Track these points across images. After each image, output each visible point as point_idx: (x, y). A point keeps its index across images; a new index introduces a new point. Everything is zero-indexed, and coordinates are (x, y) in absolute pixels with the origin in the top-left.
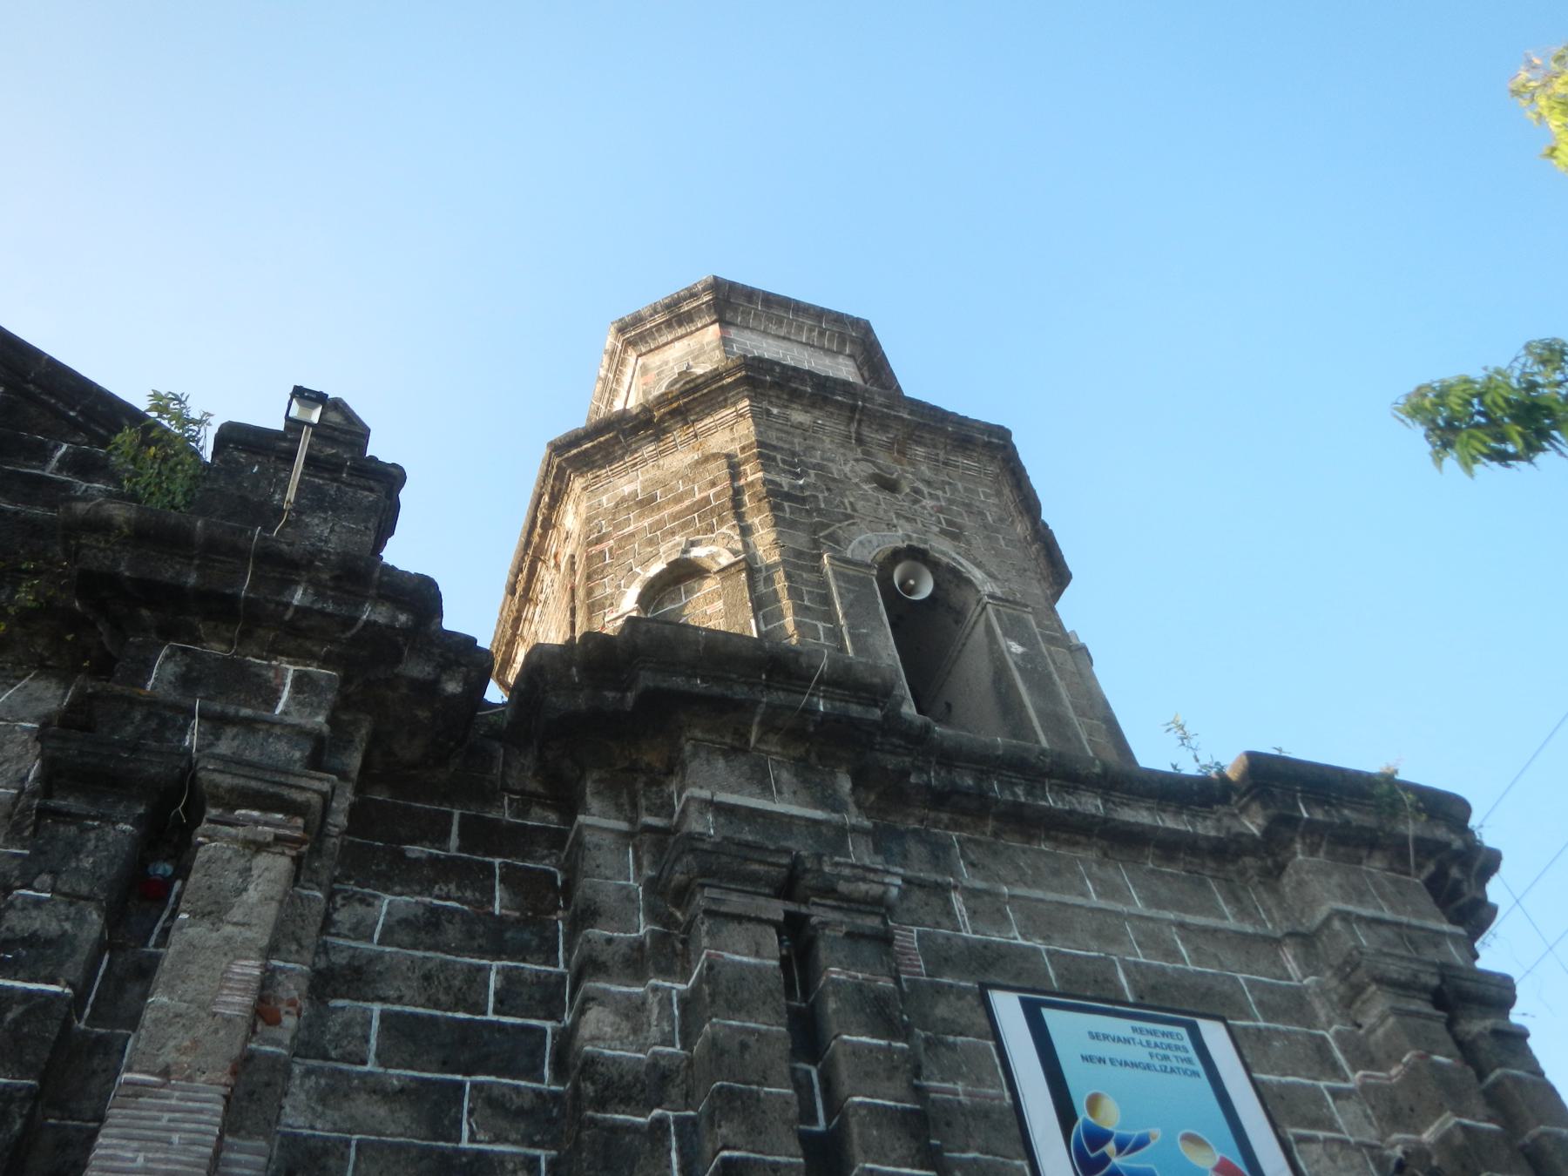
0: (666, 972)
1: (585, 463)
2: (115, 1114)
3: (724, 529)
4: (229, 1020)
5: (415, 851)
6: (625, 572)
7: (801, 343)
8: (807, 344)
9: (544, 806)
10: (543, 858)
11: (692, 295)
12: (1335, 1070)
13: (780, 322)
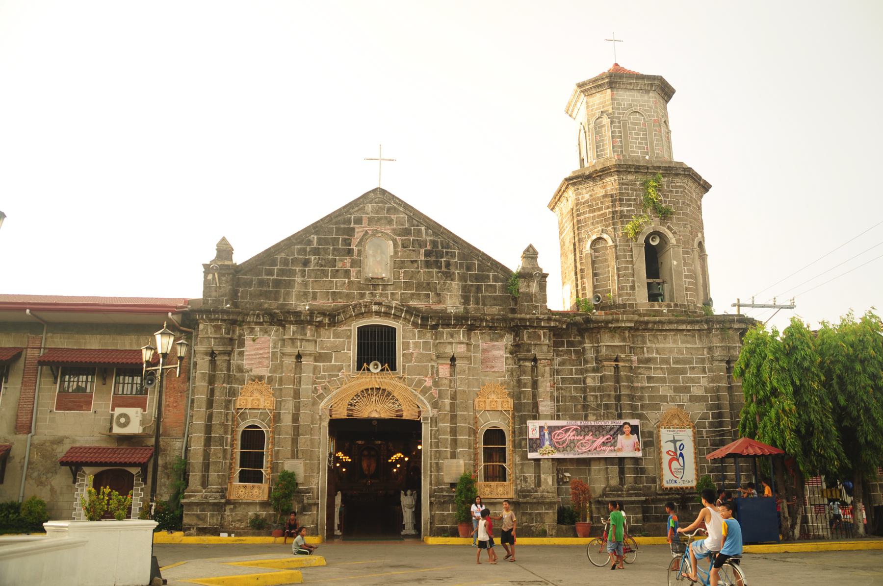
0: (598, 373)
1: (574, 184)
3: (610, 228)
11: (601, 78)
12: (705, 373)
13: (631, 84)
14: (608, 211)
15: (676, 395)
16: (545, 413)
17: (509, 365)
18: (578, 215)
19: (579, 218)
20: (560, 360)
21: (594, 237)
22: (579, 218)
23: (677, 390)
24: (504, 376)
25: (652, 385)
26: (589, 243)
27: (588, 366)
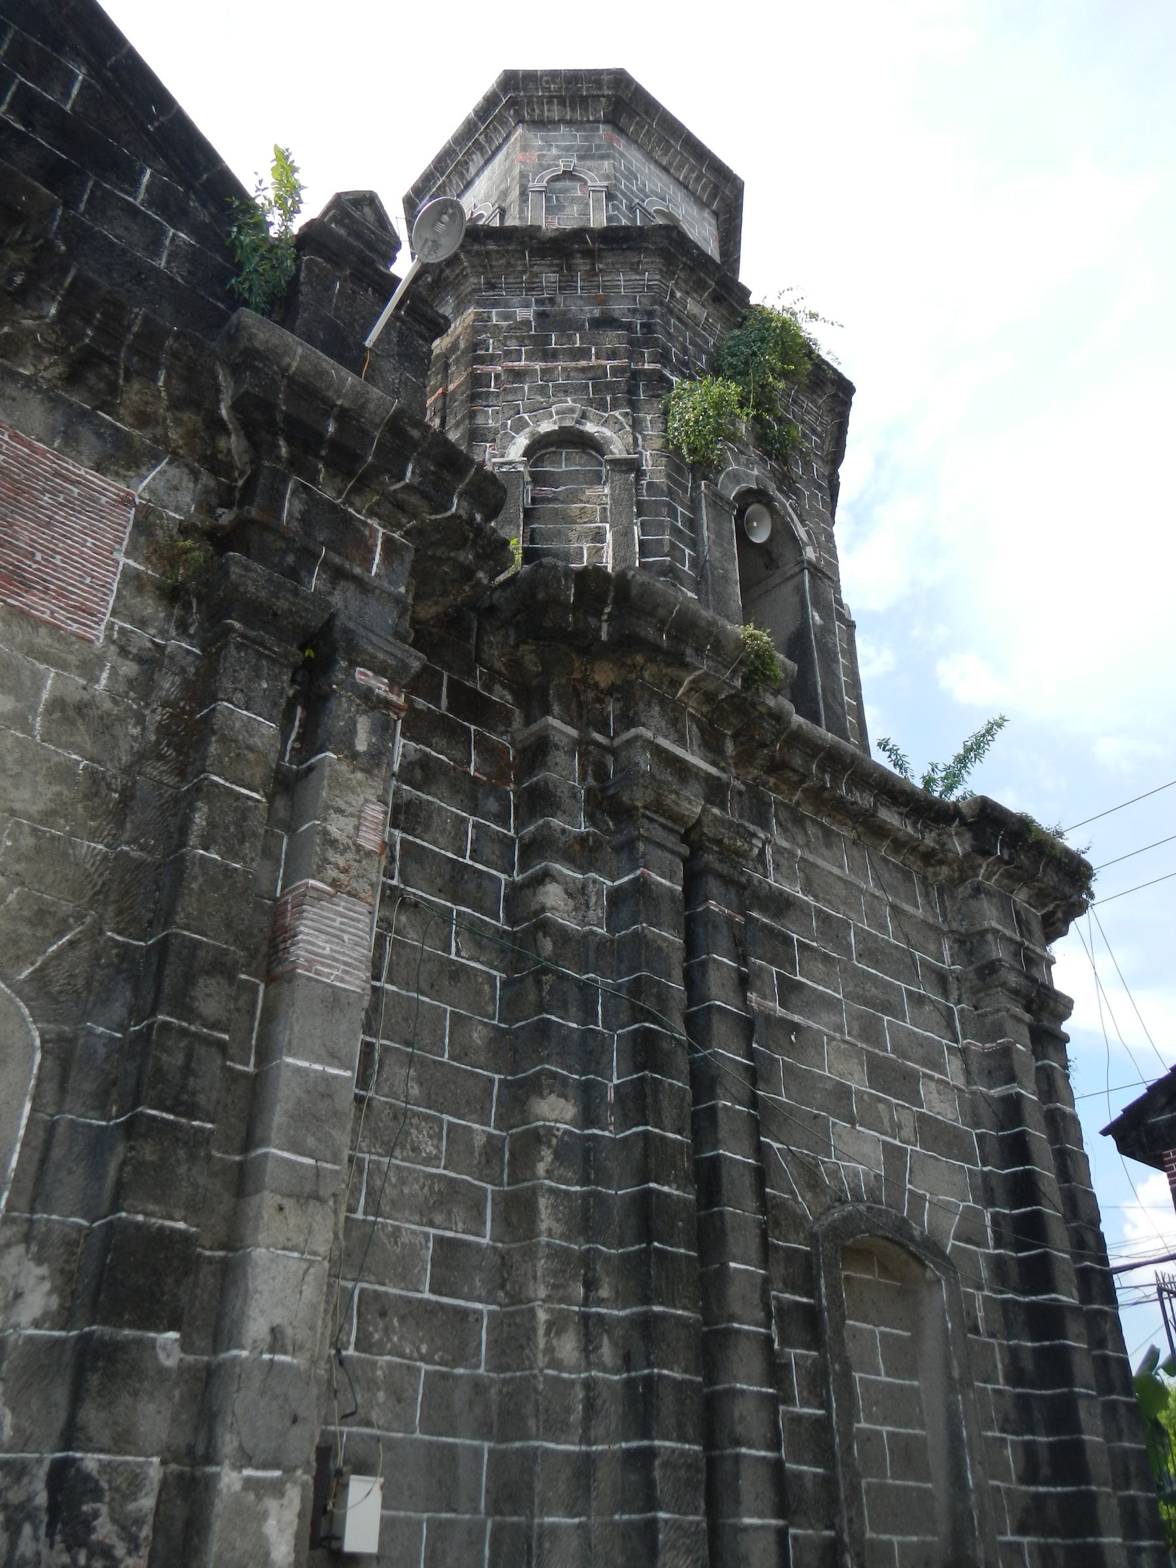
2: (310, 911)
3: (617, 413)
4: (369, 854)
5: (421, 703)
6: (512, 412)
7: (677, 180)
8: (681, 183)
9: (504, 686)
10: (502, 734)
14: (609, 364)
15: (880, 1100)
16: (331, 976)
17: (142, 623)
18: (482, 360)
19: (480, 369)
20: (413, 757)
21: (546, 427)
22: (480, 369)
23: (879, 1072)
24: (89, 668)
25: (797, 1018)
26: (522, 442)
27: (556, 822)
